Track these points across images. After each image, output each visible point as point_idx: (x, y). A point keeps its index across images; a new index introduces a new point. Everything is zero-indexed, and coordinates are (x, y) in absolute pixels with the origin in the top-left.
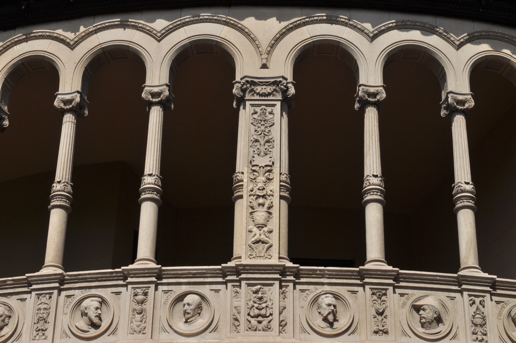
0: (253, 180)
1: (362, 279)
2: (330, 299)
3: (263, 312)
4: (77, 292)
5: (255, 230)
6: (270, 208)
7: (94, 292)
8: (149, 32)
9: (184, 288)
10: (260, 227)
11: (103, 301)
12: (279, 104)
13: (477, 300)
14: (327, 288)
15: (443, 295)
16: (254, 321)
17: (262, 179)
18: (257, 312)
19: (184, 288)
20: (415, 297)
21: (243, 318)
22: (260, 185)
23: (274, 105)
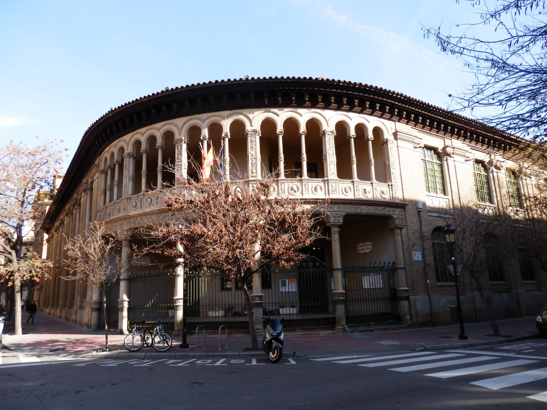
7: (294, 183)
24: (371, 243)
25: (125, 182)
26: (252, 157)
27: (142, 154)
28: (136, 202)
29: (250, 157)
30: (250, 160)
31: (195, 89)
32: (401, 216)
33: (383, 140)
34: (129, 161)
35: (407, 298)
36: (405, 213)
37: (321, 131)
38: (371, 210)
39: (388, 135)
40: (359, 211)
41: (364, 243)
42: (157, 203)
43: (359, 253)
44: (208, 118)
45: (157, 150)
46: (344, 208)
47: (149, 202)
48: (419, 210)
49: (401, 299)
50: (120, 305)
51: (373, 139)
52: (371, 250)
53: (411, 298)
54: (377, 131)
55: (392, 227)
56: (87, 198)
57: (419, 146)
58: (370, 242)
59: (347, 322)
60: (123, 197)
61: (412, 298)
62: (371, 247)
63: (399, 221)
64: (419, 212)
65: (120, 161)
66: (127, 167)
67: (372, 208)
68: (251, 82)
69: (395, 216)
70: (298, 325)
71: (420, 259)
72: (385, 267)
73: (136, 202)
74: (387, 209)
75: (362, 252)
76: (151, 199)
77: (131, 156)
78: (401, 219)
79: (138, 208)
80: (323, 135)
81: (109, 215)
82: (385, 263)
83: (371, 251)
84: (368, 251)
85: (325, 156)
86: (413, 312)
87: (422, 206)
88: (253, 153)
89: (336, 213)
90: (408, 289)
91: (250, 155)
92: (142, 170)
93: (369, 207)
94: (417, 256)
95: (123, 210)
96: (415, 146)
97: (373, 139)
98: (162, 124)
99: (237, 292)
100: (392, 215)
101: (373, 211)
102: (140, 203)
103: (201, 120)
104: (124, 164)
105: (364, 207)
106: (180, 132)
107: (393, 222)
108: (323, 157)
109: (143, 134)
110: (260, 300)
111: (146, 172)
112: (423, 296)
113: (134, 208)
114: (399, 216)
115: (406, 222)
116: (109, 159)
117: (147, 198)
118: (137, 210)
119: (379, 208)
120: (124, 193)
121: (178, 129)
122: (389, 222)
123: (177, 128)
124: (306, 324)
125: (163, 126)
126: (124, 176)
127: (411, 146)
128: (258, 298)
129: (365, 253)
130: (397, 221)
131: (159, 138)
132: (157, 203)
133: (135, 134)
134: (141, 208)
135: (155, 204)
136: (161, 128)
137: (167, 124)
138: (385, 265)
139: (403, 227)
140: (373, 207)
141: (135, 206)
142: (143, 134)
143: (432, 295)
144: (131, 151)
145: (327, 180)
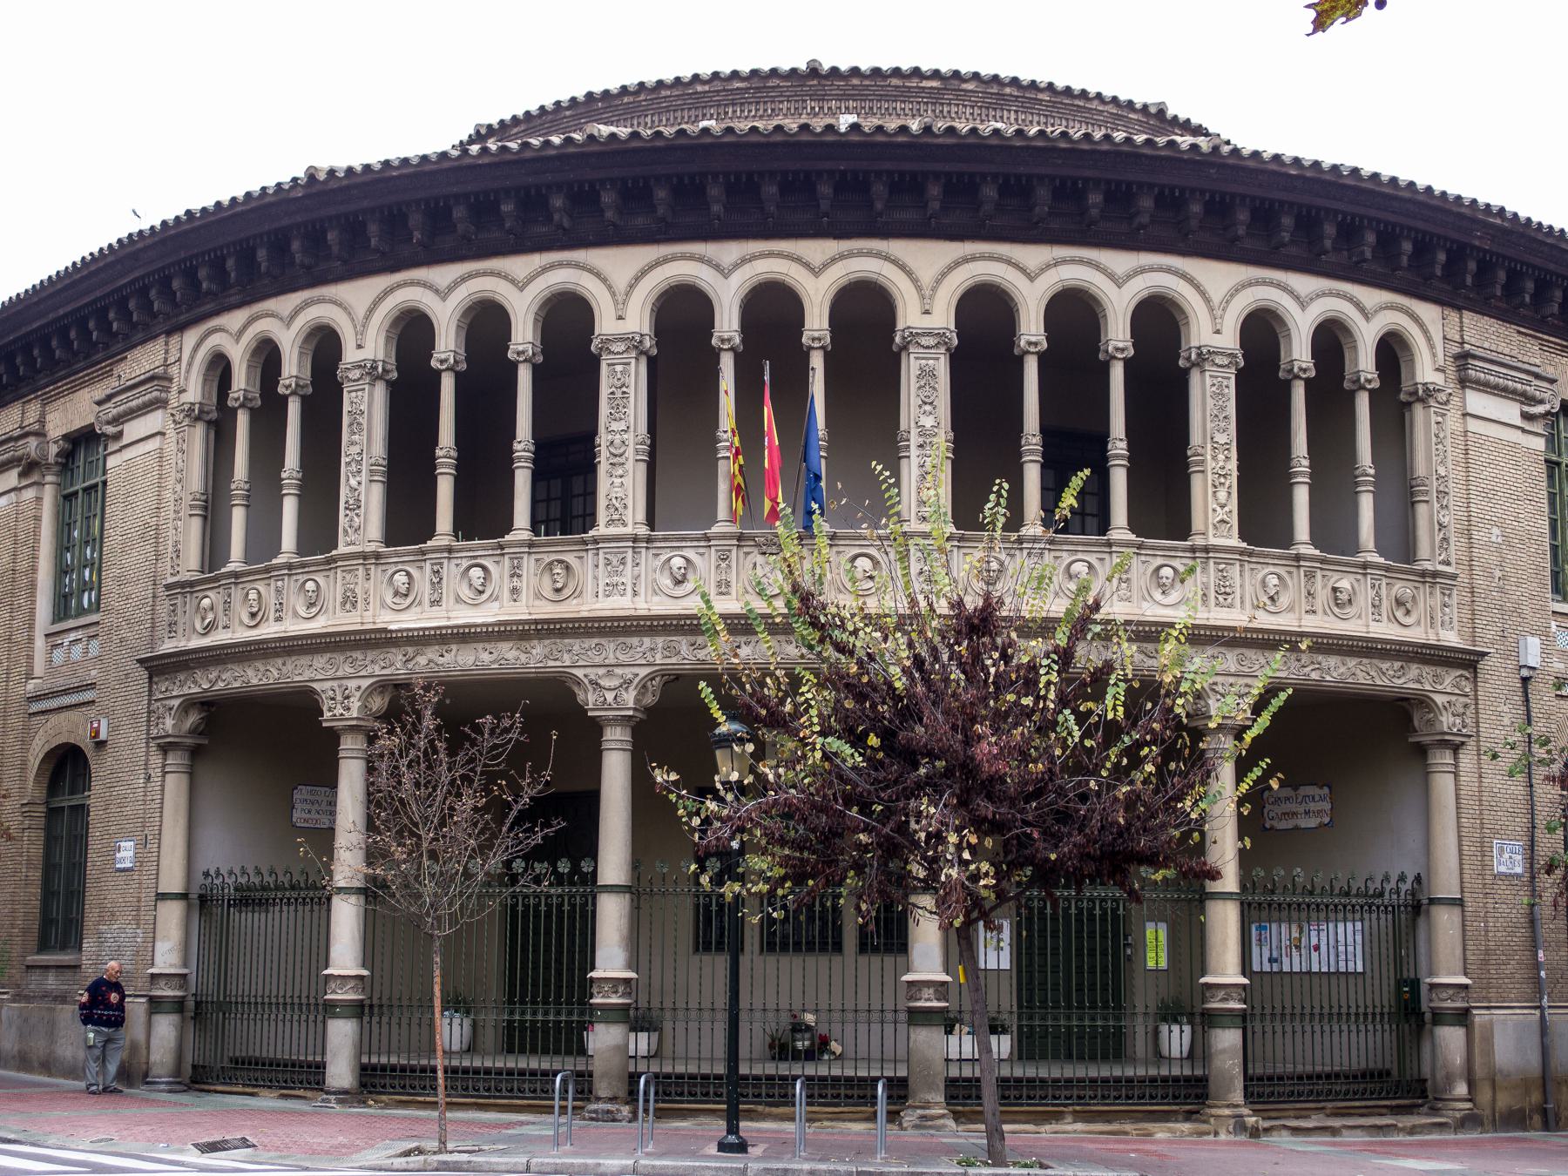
0: (1214, 458)
1: (1298, 561)
2: (1276, 581)
3: (1228, 590)
4: (1064, 554)
5: (1218, 509)
6: (1230, 487)
7: (1080, 556)
8: (1111, 276)
9: (1159, 561)
10: (1223, 506)
11: (1090, 566)
12: (1233, 377)
13: (1377, 583)
14: (1272, 569)
15: (1352, 577)
16: (1221, 598)
17: (1221, 457)
18: (1223, 590)
19: (1159, 561)
20: (1333, 580)
21: (1212, 594)
22: (1221, 464)
23: (1229, 378)
24: (1326, 790)
25: (353, 482)
26: (921, 440)
27: (438, 373)
28: (408, 574)
29: (914, 440)
30: (914, 451)
31: (712, 145)
32: (1462, 699)
33: (1411, 389)
34: (371, 395)
35: (1462, 1017)
36: (1476, 686)
37: (1184, 347)
38: (1358, 672)
39: (1427, 369)
40: (1314, 676)
41: (1296, 789)
42: (515, 591)
43: (1272, 828)
44: (744, 261)
45: (514, 366)
46: (1263, 661)
47: (477, 583)
48: (1525, 673)
49: (1439, 1018)
50: (334, 992)
51: (1376, 385)
52: (1326, 820)
53: (1477, 1019)
54: (1392, 351)
55: (1426, 739)
56: (39, 499)
57: (1540, 409)
58: (1321, 787)
59: (1248, 1094)
60: (342, 549)
61: (1480, 1017)
62: (1327, 806)
63: (1451, 719)
64: (1525, 680)
65: (306, 385)
66: (363, 420)
67: (1360, 663)
68: (940, 140)
69: (1440, 699)
70: (1067, 1098)
71: (1519, 870)
72: (1387, 894)
73: (408, 574)
74: (1414, 670)
75: (1283, 825)
76: (484, 568)
77: (379, 378)
78: (1462, 710)
79: (420, 603)
80: (1194, 365)
81: (253, 615)
82: (1387, 878)
83: (1322, 825)
84: (1312, 823)
85: (1200, 450)
86: (1480, 1071)
87: (1539, 659)
88: (928, 422)
89: (1231, 680)
90: (1468, 981)
91: (914, 432)
92: (436, 443)
93: (1352, 662)
94: (1506, 856)
95: (344, 604)
96: (1526, 409)
97: (1376, 385)
98: (537, 260)
99: (863, 960)
100: (1431, 695)
101: (1362, 678)
102: (433, 583)
103: (717, 267)
104: (346, 407)
105: (1333, 661)
106: (621, 306)
107: (1430, 723)
108: (1189, 453)
109: (443, 294)
110: (938, 1000)
111: (454, 454)
112: (1518, 1011)
113: (397, 600)
114: (1454, 698)
115: (1477, 722)
116: (244, 366)
117: (465, 563)
118: (413, 609)
119: (1385, 665)
120: (345, 531)
121: (613, 294)
122: (1416, 723)
123: (610, 287)
124: (1095, 1097)
125: (545, 270)
126: (344, 460)
127: (1510, 411)
128: (931, 991)
129: (1297, 828)
130: (1444, 719)
131: (521, 320)
132: (515, 591)
133: (399, 286)
134: (435, 603)
135: (506, 594)
136: (531, 279)
137: (561, 265)
138: (1388, 887)
139: (1463, 743)
140: (1365, 661)
141: (403, 590)
142: (443, 294)
143: (1552, 1011)
144: (381, 356)
145: (1206, 549)
